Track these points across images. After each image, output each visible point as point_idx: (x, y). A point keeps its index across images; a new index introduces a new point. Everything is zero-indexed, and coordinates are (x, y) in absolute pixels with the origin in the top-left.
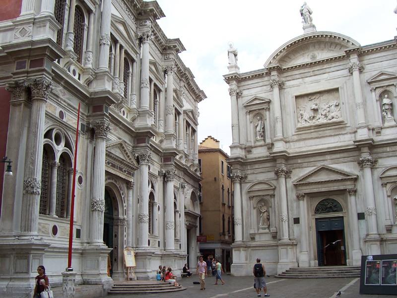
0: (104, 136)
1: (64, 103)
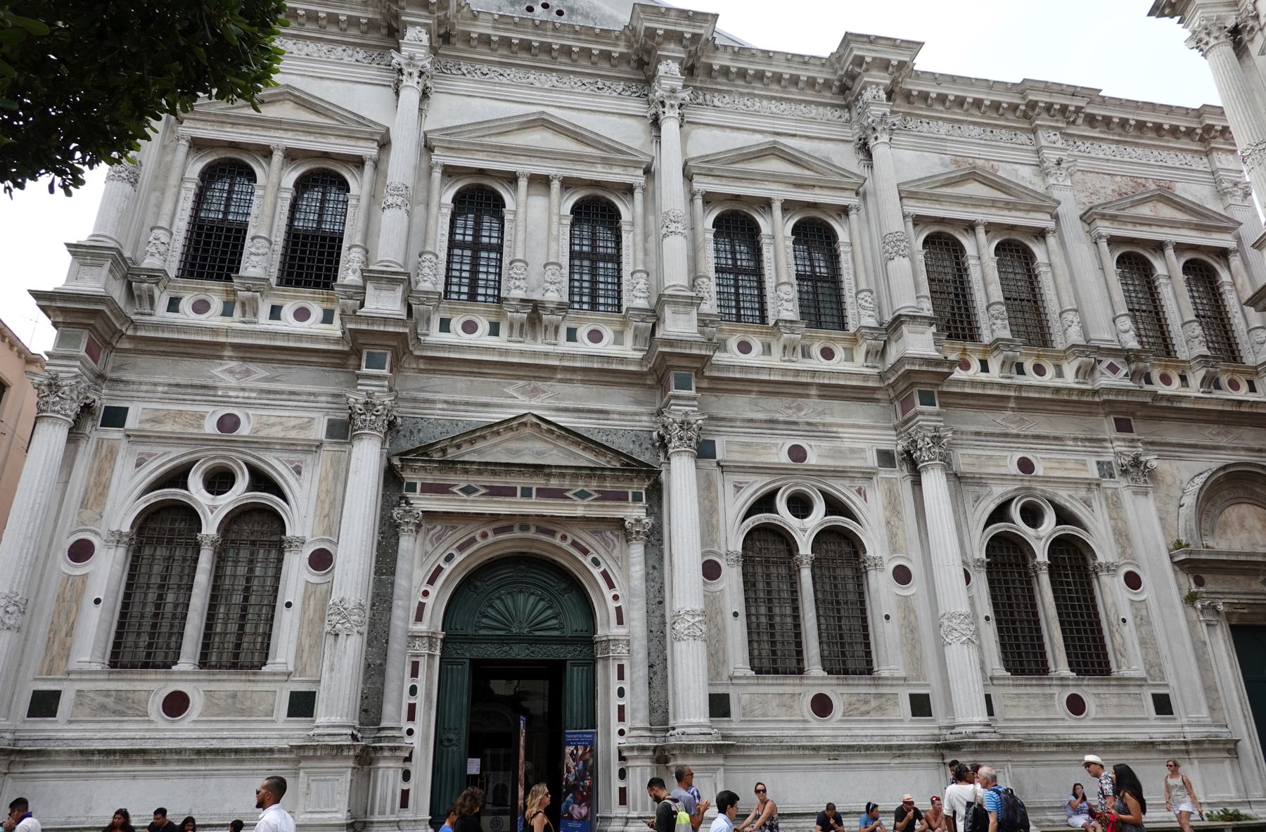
0: (359, 429)
1: (241, 394)
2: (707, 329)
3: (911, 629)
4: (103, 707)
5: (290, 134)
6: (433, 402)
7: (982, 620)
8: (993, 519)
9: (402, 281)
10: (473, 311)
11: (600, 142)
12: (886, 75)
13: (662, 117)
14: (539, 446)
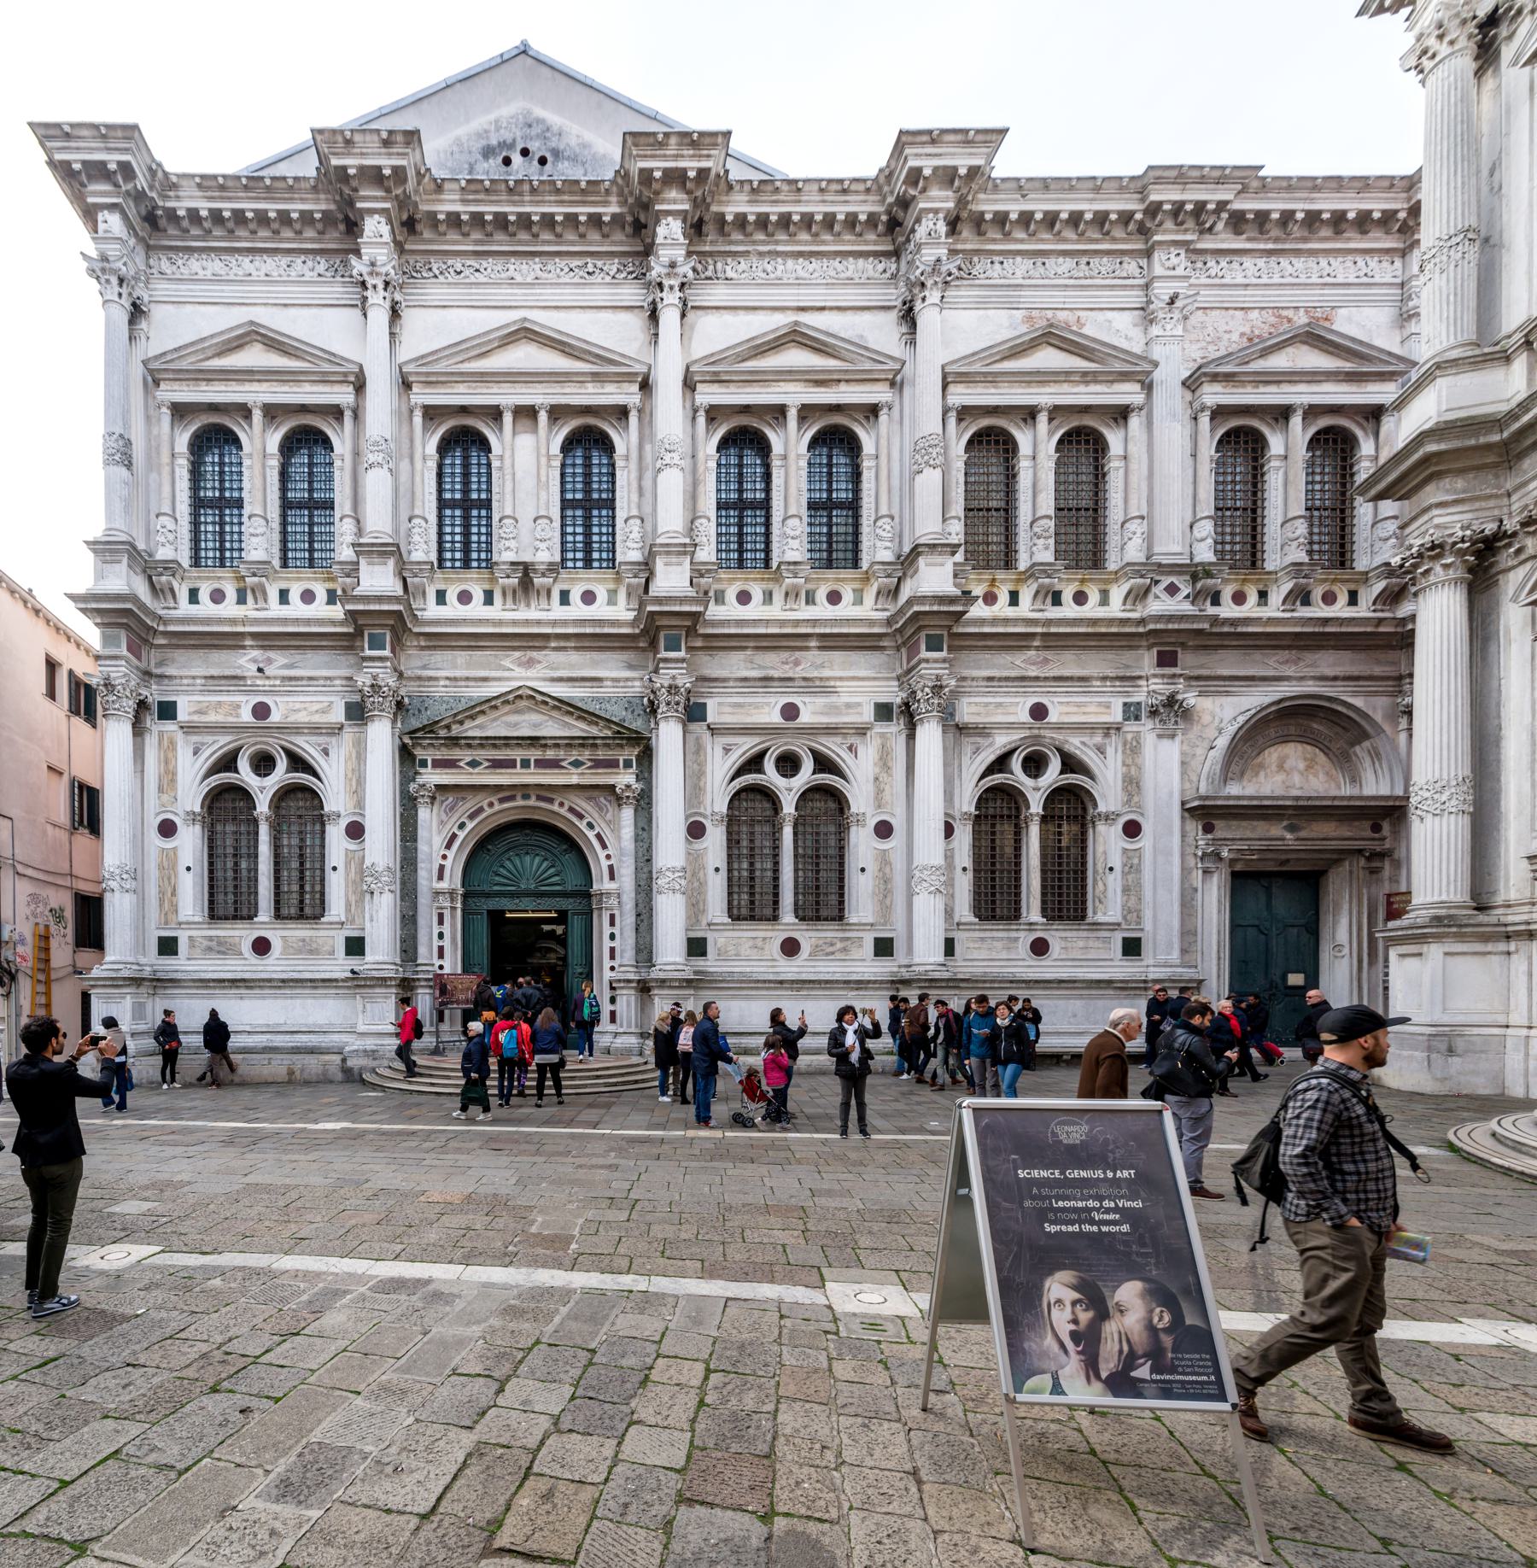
2: (703, 581)
3: (885, 881)
4: (210, 949)
5: (265, 386)
6: (436, 679)
7: (959, 870)
8: (990, 771)
9: (392, 553)
10: (467, 580)
11: (590, 353)
12: (950, 193)
13: (660, 306)
14: (535, 717)
